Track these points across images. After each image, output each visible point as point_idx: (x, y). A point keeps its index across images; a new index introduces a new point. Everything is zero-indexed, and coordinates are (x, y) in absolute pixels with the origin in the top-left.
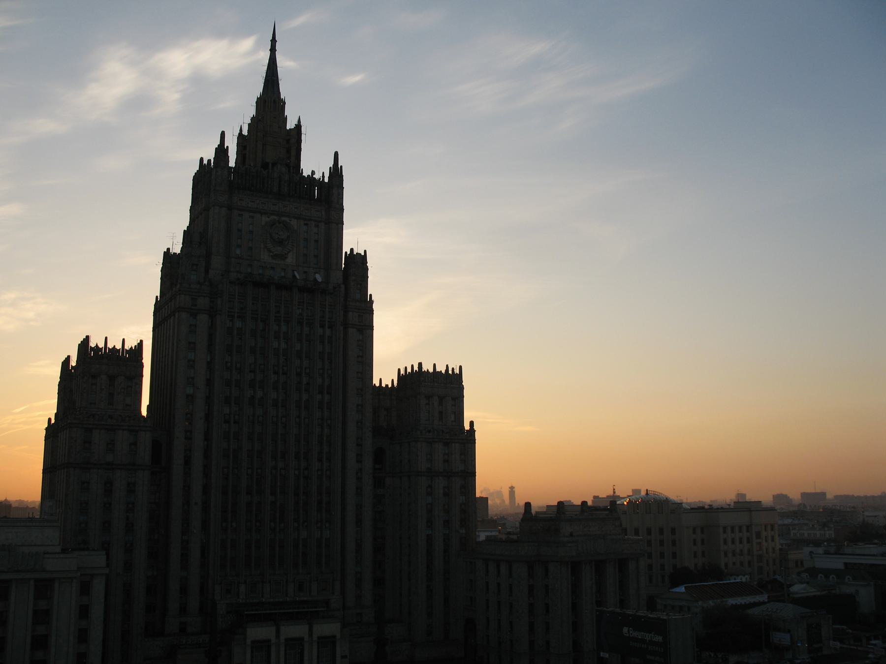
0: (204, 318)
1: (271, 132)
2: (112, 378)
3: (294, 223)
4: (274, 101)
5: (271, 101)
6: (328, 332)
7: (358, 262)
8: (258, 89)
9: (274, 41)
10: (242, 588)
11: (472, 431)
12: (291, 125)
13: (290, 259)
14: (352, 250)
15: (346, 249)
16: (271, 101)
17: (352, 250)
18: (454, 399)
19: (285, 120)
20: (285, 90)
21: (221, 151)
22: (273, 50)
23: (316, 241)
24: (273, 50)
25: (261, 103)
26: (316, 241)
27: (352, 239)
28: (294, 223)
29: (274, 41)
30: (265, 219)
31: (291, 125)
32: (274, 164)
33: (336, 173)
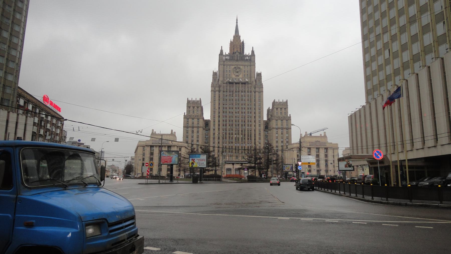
0: (217, 93)
1: (237, 45)
2: (194, 107)
3: (241, 67)
5: (237, 36)
6: (249, 94)
7: (259, 75)
9: (237, 20)
10: (227, 157)
11: (290, 117)
12: (242, 41)
13: (241, 76)
16: (237, 36)
18: (285, 109)
20: (240, 34)
22: (237, 22)
24: (237, 22)
27: (258, 69)
28: (241, 67)
29: (237, 20)
30: (233, 67)
31: (242, 41)
33: (253, 52)
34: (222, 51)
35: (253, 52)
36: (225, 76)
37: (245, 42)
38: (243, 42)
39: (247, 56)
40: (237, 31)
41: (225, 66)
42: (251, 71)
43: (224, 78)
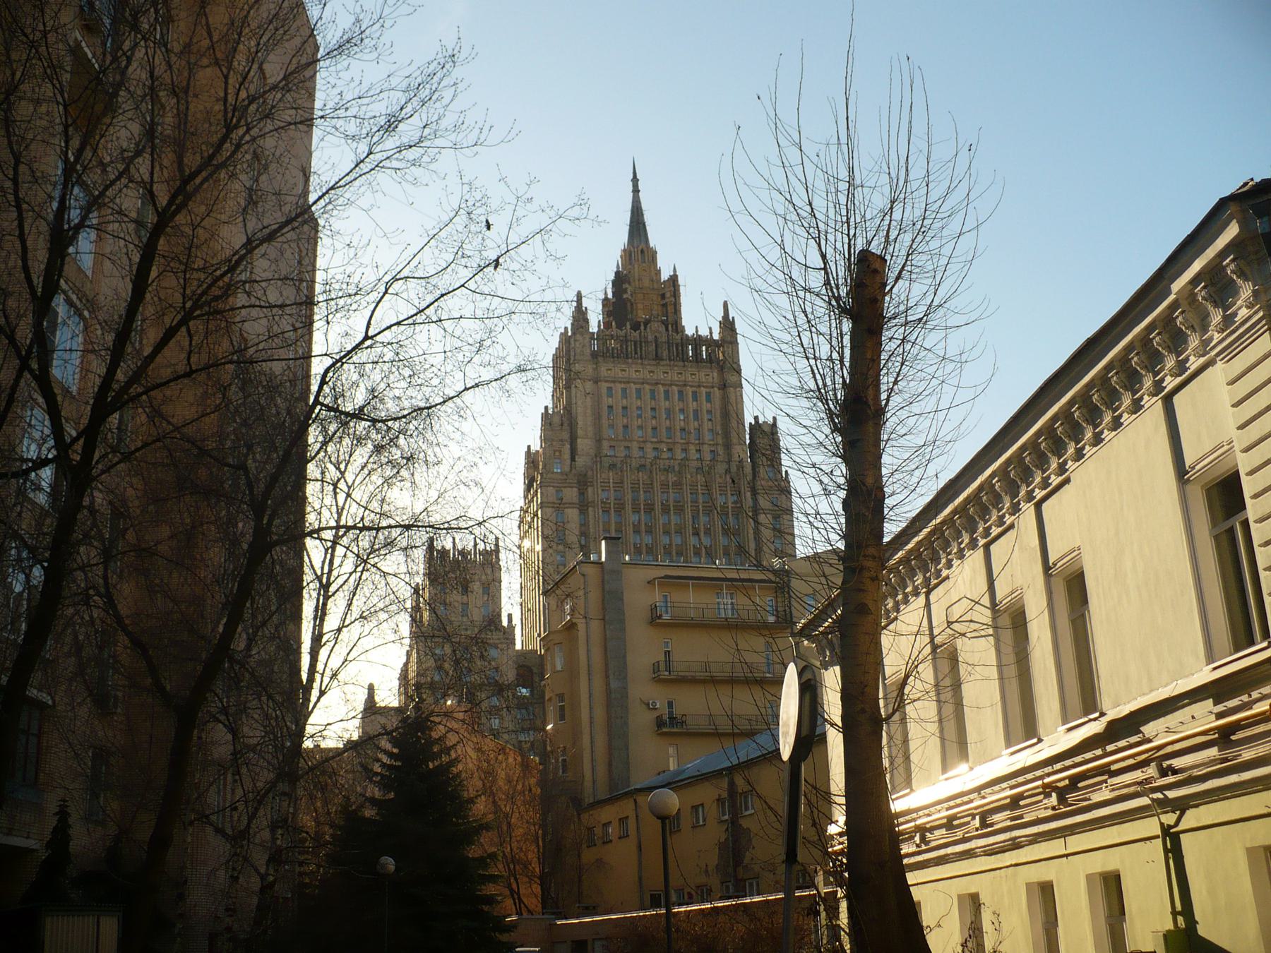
0: (573, 514)
4: (642, 251)
8: (621, 237)
9: (635, 180)
12: (665, 275)
14: (756, 418)
15: (749, 419)
17: (756, 418)
19: (658, 272)
20: (655, 238)
21: (580, 316)
22: (636, 191)
23: (709, 412)
24: (636, 191)
25: (628, 255)
26: (709, 412)
29: (635, 180)
31: (665, 275)
32: (647, 323)
33: (728, 325)
34: (580, 316)
35: (728, 325)
36: (608, 433)
37: (681, 281)
38: (674, 279)
39: (698, 341)
40: (637, 225)
41: (604, 386)
42: (726, 415)
43: (599, 441)
